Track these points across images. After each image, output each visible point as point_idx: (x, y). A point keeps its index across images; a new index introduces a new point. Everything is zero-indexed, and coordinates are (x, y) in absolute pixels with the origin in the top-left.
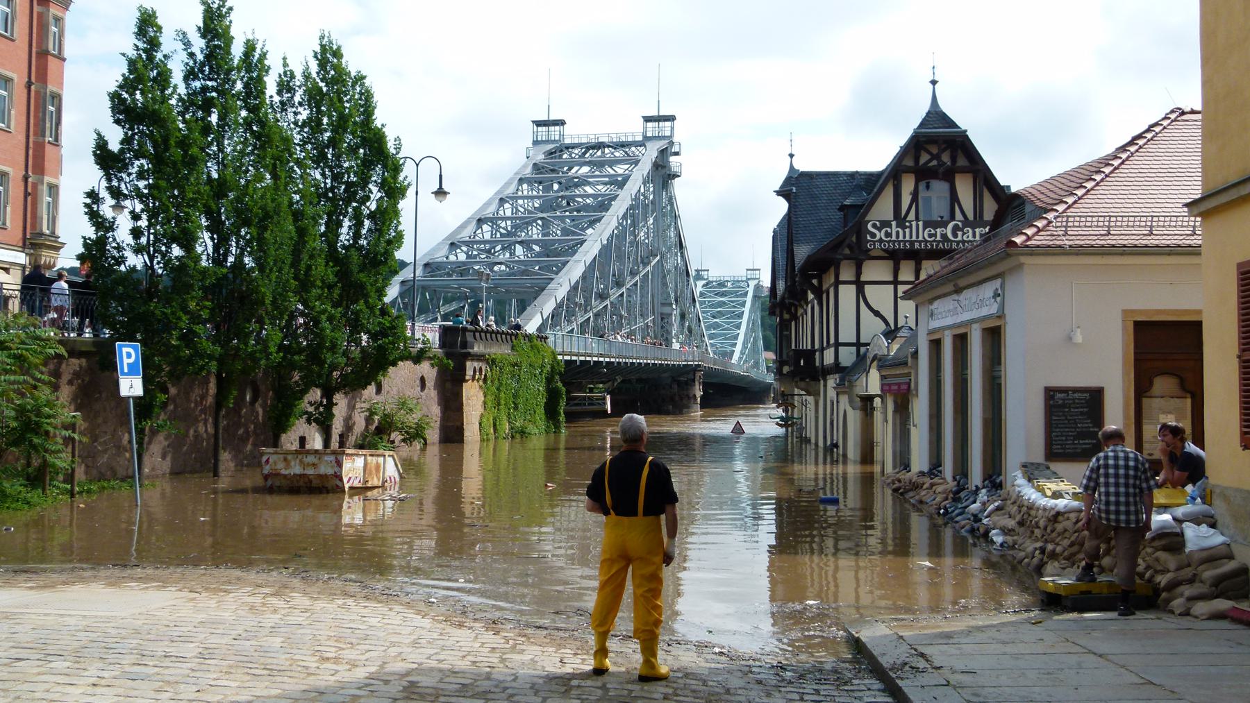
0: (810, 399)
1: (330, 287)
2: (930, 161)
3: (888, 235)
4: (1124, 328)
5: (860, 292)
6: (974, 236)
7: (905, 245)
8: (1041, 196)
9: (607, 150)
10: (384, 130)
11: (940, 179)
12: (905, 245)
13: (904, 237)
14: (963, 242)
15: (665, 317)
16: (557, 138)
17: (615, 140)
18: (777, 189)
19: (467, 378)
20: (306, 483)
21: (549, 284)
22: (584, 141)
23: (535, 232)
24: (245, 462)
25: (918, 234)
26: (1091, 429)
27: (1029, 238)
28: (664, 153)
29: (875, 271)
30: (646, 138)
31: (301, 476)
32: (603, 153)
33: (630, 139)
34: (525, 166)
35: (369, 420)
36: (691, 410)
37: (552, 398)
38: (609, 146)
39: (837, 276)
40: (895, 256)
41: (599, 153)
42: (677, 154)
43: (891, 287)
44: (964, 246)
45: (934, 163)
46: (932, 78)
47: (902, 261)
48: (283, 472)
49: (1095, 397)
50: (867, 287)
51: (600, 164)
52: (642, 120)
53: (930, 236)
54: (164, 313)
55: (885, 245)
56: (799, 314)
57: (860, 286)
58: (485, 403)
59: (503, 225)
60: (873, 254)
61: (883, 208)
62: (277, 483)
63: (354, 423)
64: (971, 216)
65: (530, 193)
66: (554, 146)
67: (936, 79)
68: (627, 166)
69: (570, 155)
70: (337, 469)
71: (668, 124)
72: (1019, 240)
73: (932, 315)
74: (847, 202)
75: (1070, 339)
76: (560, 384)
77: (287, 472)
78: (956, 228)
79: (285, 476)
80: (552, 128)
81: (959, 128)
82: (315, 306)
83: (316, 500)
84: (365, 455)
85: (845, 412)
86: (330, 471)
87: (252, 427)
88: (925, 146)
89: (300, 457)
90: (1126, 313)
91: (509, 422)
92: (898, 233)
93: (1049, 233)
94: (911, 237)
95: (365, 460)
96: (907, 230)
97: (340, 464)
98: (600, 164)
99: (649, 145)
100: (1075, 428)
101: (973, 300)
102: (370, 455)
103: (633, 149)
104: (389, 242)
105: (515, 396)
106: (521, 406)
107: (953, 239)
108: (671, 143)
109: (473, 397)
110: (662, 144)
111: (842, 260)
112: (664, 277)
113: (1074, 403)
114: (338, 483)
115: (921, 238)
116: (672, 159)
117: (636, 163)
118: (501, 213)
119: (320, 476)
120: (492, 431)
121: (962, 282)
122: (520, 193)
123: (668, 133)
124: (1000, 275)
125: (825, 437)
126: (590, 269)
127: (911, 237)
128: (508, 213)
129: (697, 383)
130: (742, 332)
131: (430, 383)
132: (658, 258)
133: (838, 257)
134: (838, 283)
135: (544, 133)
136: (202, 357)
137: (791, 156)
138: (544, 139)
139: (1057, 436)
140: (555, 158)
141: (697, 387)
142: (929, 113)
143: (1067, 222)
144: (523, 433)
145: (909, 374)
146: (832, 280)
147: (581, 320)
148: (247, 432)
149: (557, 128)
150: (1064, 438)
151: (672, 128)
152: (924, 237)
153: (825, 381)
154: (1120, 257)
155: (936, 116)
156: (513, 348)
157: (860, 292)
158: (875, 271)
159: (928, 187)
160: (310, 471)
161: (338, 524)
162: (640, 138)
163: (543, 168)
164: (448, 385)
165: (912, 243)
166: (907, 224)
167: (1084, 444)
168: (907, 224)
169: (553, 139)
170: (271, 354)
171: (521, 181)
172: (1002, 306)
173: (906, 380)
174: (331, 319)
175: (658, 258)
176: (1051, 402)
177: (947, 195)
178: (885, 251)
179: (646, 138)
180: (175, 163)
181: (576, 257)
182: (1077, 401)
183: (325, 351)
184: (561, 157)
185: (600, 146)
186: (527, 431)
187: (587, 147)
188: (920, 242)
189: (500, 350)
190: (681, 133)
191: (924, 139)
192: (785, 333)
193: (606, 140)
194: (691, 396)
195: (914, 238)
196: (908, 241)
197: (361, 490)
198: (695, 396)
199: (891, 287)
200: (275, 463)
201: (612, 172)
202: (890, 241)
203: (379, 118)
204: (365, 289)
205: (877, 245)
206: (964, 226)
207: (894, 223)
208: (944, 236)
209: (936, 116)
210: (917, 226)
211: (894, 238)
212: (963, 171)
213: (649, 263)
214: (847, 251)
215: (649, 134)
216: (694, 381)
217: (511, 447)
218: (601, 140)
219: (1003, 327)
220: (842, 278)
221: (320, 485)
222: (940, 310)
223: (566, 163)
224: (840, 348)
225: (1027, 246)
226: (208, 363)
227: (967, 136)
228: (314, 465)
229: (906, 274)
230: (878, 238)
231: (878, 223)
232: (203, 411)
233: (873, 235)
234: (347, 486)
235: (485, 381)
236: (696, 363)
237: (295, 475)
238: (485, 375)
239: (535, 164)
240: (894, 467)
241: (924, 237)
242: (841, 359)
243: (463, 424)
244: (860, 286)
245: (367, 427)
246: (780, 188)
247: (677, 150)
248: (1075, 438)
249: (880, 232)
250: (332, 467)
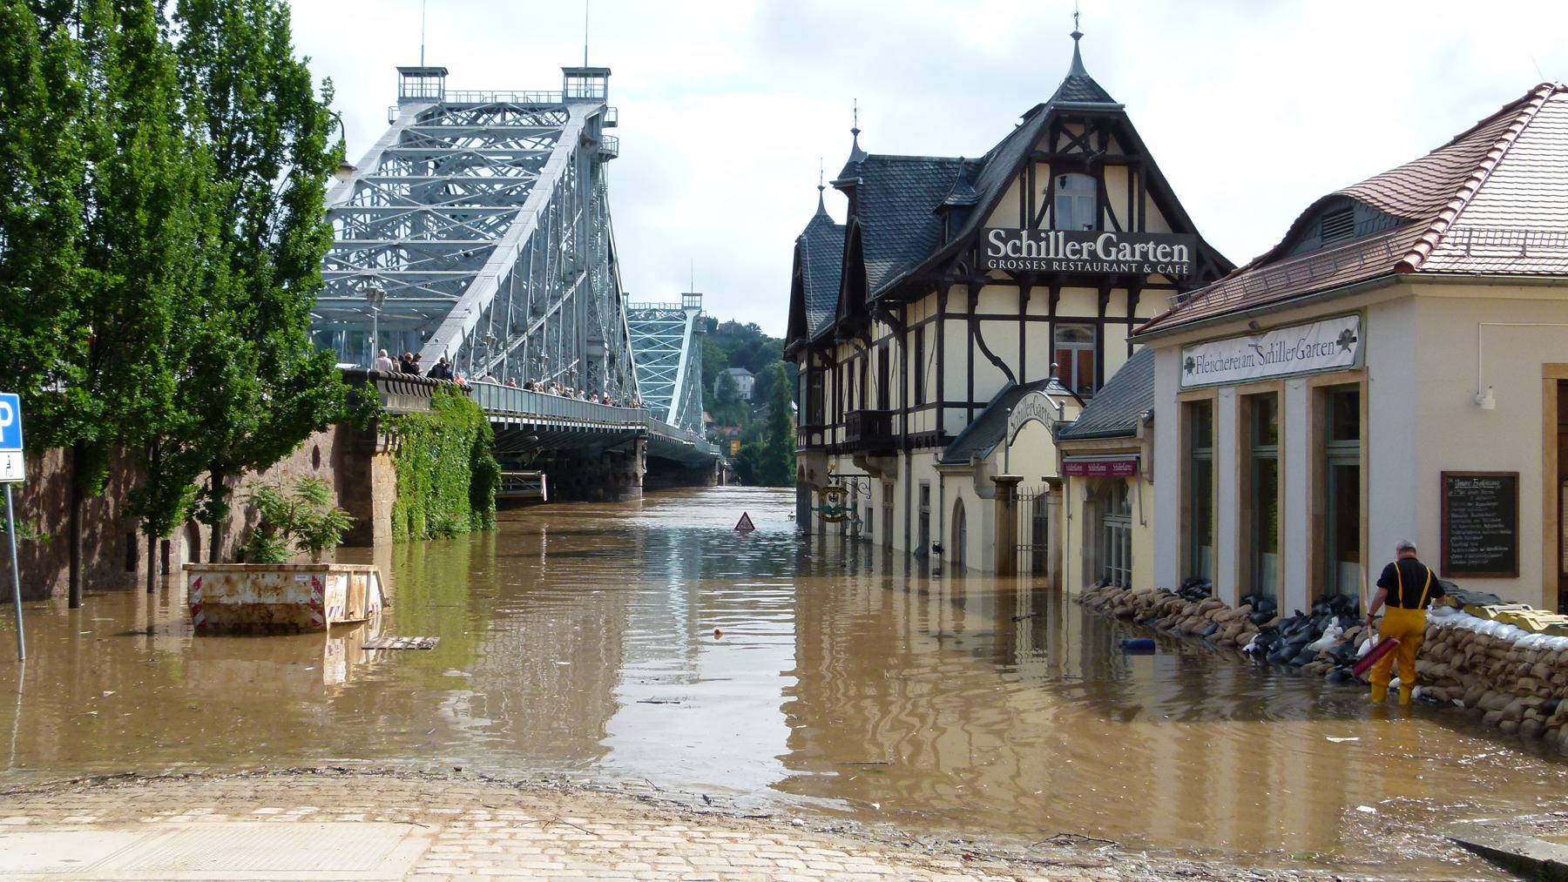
0: (875, 481)
1: (240, 307)
2: (1070, 147)
3: (1017, 249)
4: (1546, 390)
5: (974, 330)
6: (1133, 254)
7: (1040, 266)
8: (1387, 200)
9: (509, 116)
10: (308, 66)
11: (1087, 174)
12: (1040, 266)
13: (1039, 253)
14: (1118, 262)
15: (592, 361)
16: (435, 94)
17: (521, 101)
18: (835, 179)
19: (379, 448)
20: (262, 618)
21: (451, 309)
22: (476, 100)
23: (403, 233)
24: (91, 582)
25: (1058, 250)
26: (1502, 532)
27: (1423, 260)
28: (594, 122)
29: (996, 300)
30: (567, 100)
31: (255, 606)
32: (503, 118)
33: (544, 100)
34: (389, 135)
35: (249, 514)
36: (629, 495)
37: (480, 481)
38: (512, 110)
39: (942, 305)
40: (1023, 280)
41: (498, 119)
42: (612, 124)
43: (1017, 323)
44: (1119, 267)
45: (1077, 150)
46: (1073, 30)
47: (1033, 288)
48: (225, 600)
49: (1508, 485)
50: (982, 323)
51: (500, 135)
52: (562, 74)
53: (1074, 252)
54: (23, 345)
55: (1012, 264)
56: (840, 360)
57: (974, 321)
58: (398, 486)
59: (361, 219)
60: (1151, 280)
61: (1008, 213)
62: (215, 619)
63: (231, 519)
64: (1125, 227)
65: (396, 174)
66: (431, 105)
67: (1080, 31)
68: (538, 140)
69: (455, 121)
70: (314, 595)
71: (600, 81)
72: (1413, 260)
73: (1190, 365)
74: (950, 201)
75: (1477, 404)
76: (490, 458)
77: (230, 601)
78: (1108, 244)
79: (228, 607)
80: (427, 80)
81: (1114, 101)
82: (219, 337)
83: (279, 645)
84: (348, 573)
85: (959, 503)
86: (303, 599)
87: (100, 526)
88: (1069, 127)
89: (252, 576)
90: (1548, 368)
91: (427, 515)
92: (1030, 247)
93: (1445, 252)
94: (1048, 253)
95: (349, 580)
96: (1043, 244)
97: (320, 589)
98: (500, 135)
99: (572, 110)
100: (1480, 529)
101: (1290, 344)
102: (356, 573)
103: (548, 115)
104: (315, 240)
105: (435, 476)
106: (441, 491)
107: (1101, 255)
108: (604, 109)
109: (383, 473)
110: (592, 109)
111: (951, 283)
112: (593, 303)
113: (1480, 495)
114: (317, 617)
115: (1061, 256)
116: (605, 131)
117: (556, 136)
118: (358, 202)
119: (288, 606)
120: (406, 529)
121: (1264, 322)
122: (384, 175)
123: (599, 94)
124: (1359, 312)
125: (908, 537)
126: (505, 286)
127: (1048, 253)
128: (368, 204)
129: (639, 457)
130: (678, 383)
131: (325, 458)
132: (584, 275)
133: (947, 279)
134: (942, 316)
135: (415, 87)
136: (77, 418)
137: (856, 132)
138: (415, 95)
139: (1457, 542)
140: (432, 124)
141: (639, 462)
142: (1069, 80)
143: (1470, 237)
144: (448, 530)
145: (1137, 450)
146: (933, 310)
147: (493, 363)
148: (93, 534)
149: (435, 80)
150: (1466, 545)
152: (1065, 255)
153: (909, 456)
154: (1548, 289)
155: (1079, 83)
156: (432, 406)
157: (974, 330)
158: (996, 300)
159: (1063, 184)
160: (270, 599)
161: (319, 679)
162: (558, 100)
163: (417, 138)
164: (349, 460)
165: (1049, 262)
166: (1043, 235)
167: (1492, 552)
168: (1043, 235)
169: (428, 95)
170: (166, 412)
171: (386, 156)
172: (1362, 352)
173: (1132, 457)
174: (240, 357)
175: (584, 275)
176: (1450, 493)
177: (1092, 195)
178: (1008, 271)
179: (567, 100)
180: (38, 102)
181: (486, 270)
182: (1483, 492)
183: (232, 408)
184: (439, 123)
185: (500, 108)
186: (455, 528)
187: (480, 110)
188: (1060, 261)
189: (416, 408)
190: (620, 96)
191: (1066, 116)
192: (816, 386)
193: (508, 100)
194: (630, 474)
195: (1052, 255)
196: (1043, 259)
197: (343, 628)
198: (636, 475)
199: (1017, 323)
200: (211, 586)
201: (516, 148)
202: (1019, 259)
203: (301, 46)
204: (282, 311)
205: (1002, 265)
206: (1120, 240)
207: (1024, 233)
208: (1093, 253)
209: (1079, 83)
210: (1057, 238)
211: (1024, 254)
212: (1115, 162)
213: (574, 282)
214: (957, 272)
215: (572, 94)
216: (634, 453)
217: (429, 547)
218: (500, 100)
219: (1362, 390)
220: (949, 310)
221: (286, 621)
222: (1208, 359)
223: (444, 132)
224: (946, 410)
225: (1424, 271)
226: (81, 427)
227: (1125, 113)
228: (276, 588)
229: (1038, 306)
230: (1002, 254)
231: (1002, 233)
232: (35, 502)
233: (996, 250)
234: (329, 621)
235: (398, 454)
236: (639, 428)
237: (245, 606)
238: (400, 446)
239: (404, 132)
240: (1086, 582)
241: (1065, 255)
242: (947, 425)
243: (371, 519)
244: (974, 321)
245: (247, 525)
246: (840, 177)
247: (612, 119)
248: (1481, 544)
249: (1006, 245)
250: (308, 592)
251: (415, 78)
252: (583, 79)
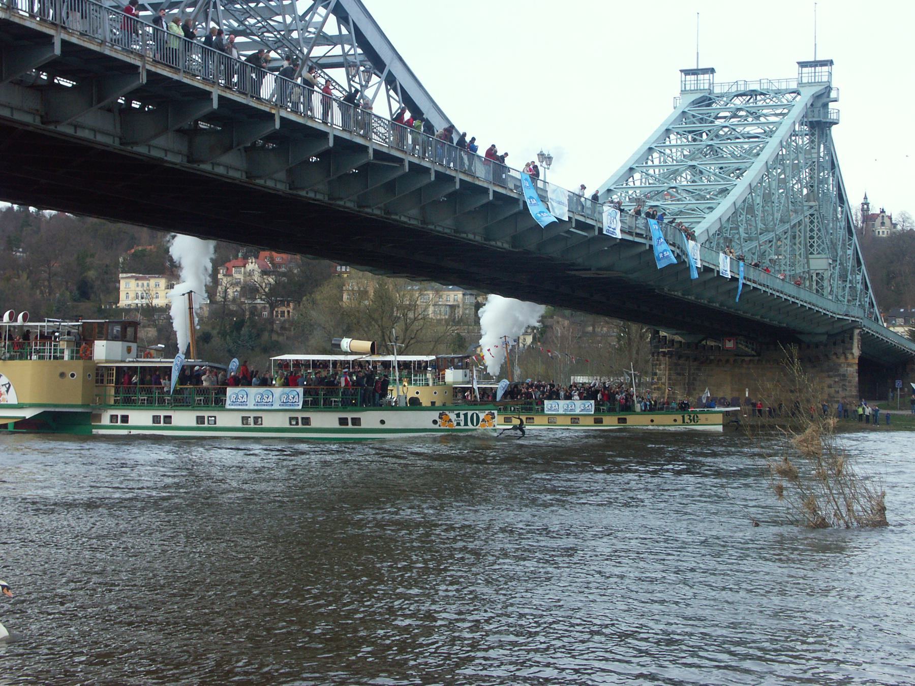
16: (706, 87)
33: (783, 86)
38: (762, 94)
71: (825, 69)
80: (701, 77)
108: (829, 89)
123: (825, 79)
135: (693, 82)
149: (707, 76)
162: (793, 86)
169: (702, 88)
215: (805, 80)
251: (693, 76)
252: (813, 68)
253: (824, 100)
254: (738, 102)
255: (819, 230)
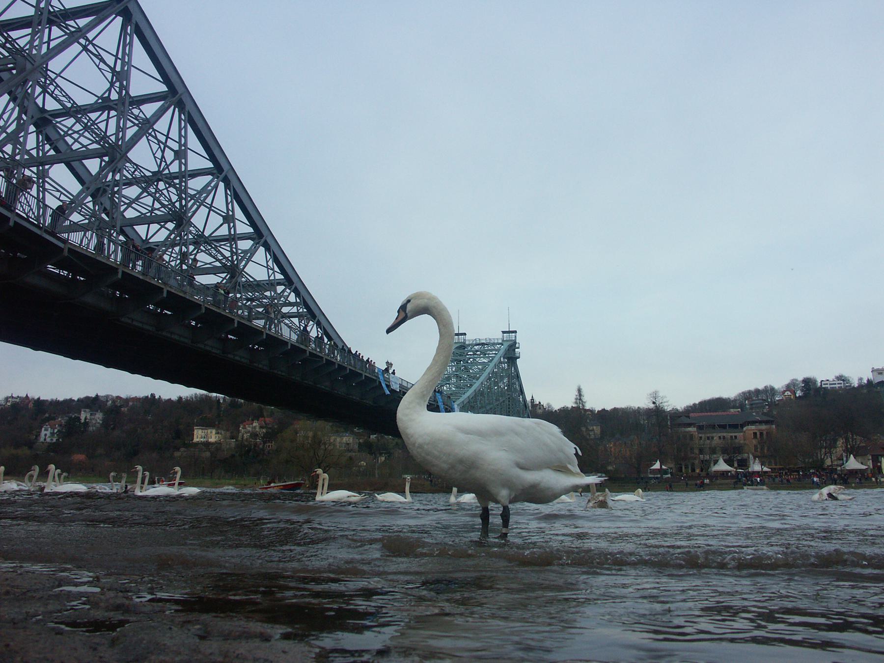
33: (496, 342)
38: (487, 345)
42: (518, 348)
71: (513, 334)
80: (460, 337)
108: (515, 343)
123: (514, 339)
151: (516, 337)
162: (500, 341)
253: (513, 348)
254: (476, 347)
255: (512, 405)
